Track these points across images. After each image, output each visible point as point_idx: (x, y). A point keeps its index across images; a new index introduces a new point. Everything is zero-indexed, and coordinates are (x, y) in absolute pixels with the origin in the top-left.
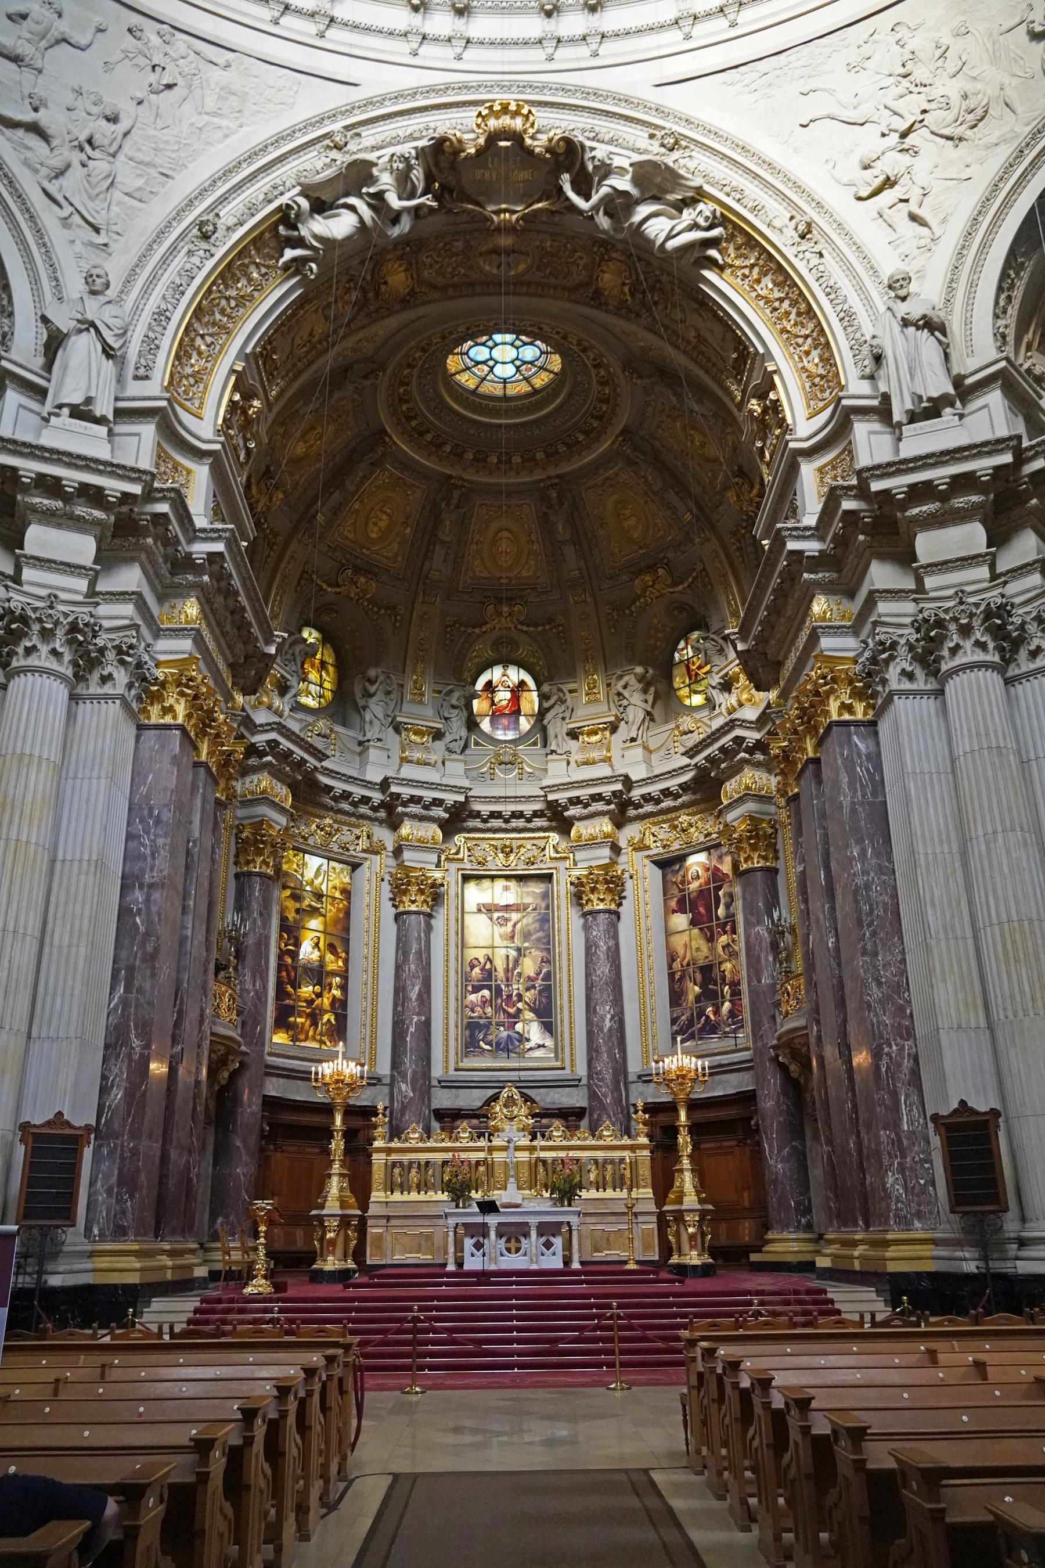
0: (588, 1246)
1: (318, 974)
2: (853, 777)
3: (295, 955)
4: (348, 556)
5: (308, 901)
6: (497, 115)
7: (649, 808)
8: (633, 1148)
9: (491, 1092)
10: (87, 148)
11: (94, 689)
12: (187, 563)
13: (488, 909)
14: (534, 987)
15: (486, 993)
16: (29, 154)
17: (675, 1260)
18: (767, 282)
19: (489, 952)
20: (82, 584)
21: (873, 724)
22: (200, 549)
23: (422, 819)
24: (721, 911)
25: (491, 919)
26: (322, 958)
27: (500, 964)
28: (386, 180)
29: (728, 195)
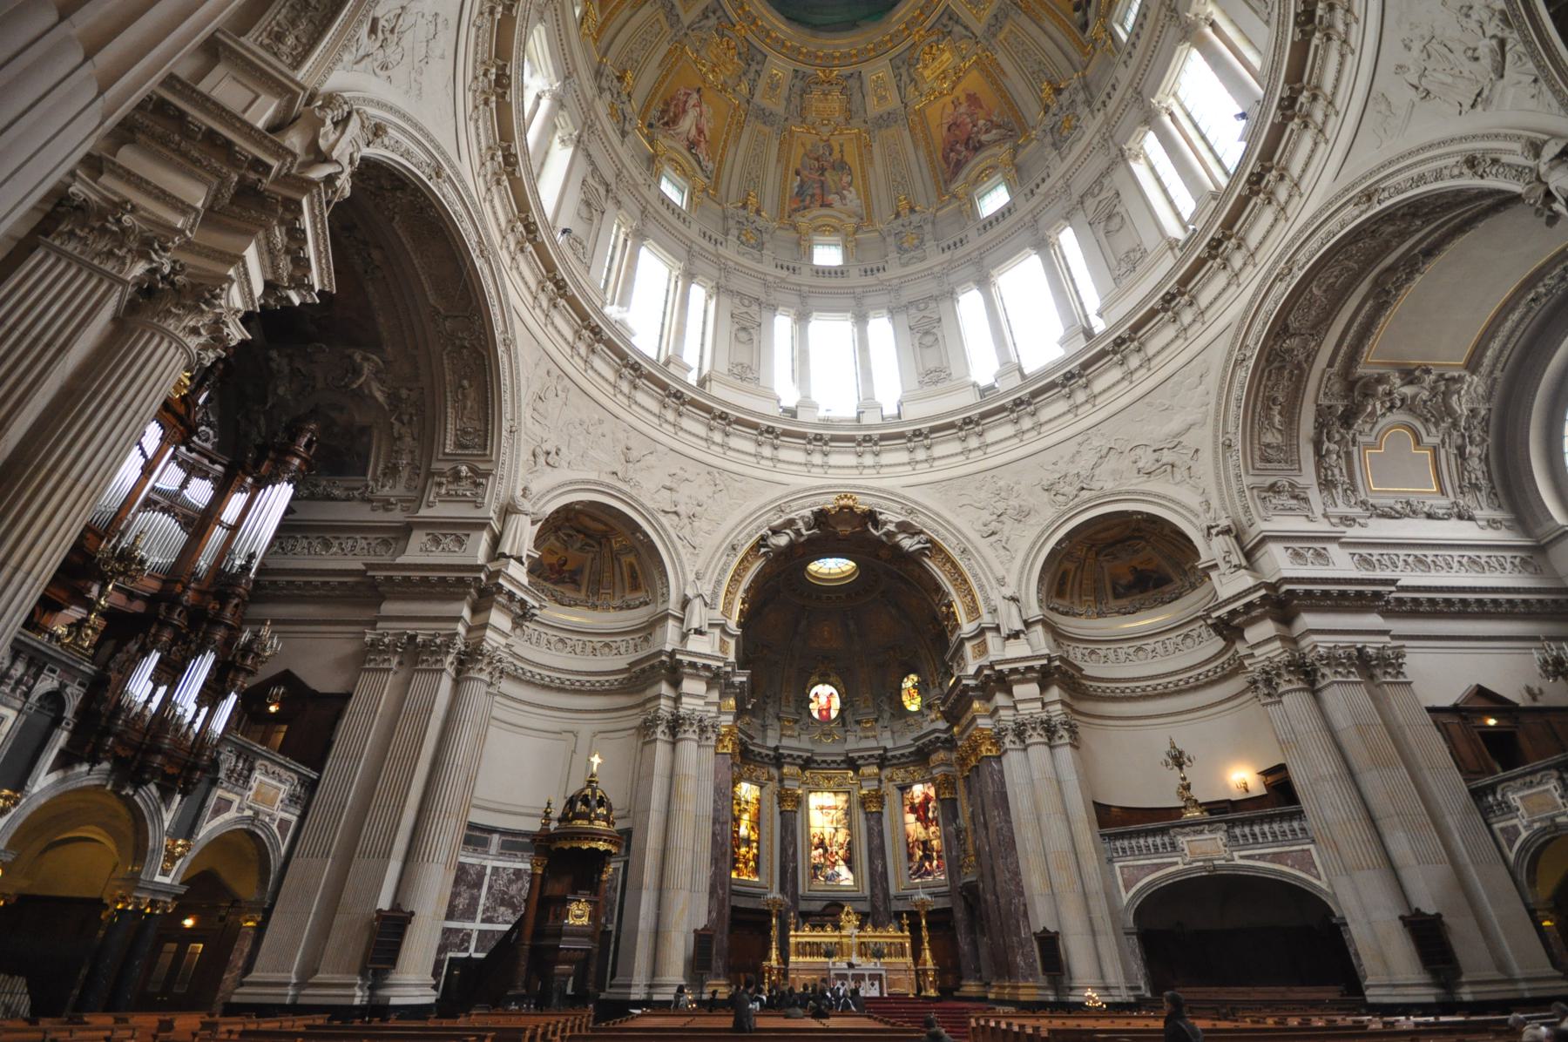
0: (889, 987)
2: (993, 779)
3: (738, 832)
5: (743, 805)
7: (895, 761)
8: (902, 937)
9: (825, 903)
11: (704, 743)
12: (732, 685)
13: (822, 808)
15: (821, 850)
17: (923, 994)
18: (948, 565)
20: (702, 702)
21: (999, 758)
24: (930, 815)
28: (800, 524)
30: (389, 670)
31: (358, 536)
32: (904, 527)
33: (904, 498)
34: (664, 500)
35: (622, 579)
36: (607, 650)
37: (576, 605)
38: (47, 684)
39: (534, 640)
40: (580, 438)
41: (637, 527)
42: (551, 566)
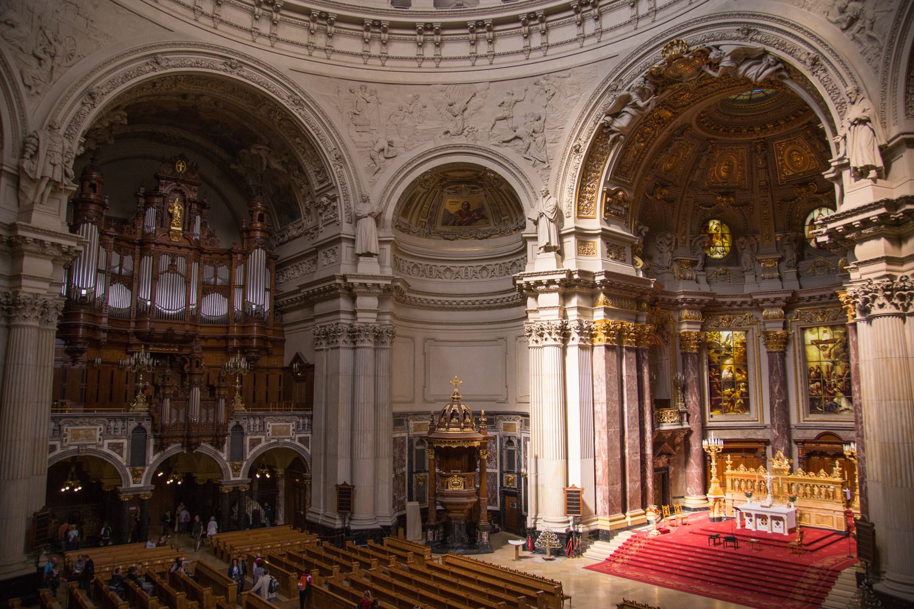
1: (732, 383)
3: (719, 377)
4: (715, 190)
6: (671, 48)
9: (822, 431)
10: (534, 134)
13: (817, 343)
14: (842, 380)
15: (818, 384)
16: (517, 147)
19: (818, 364)
22: (598, 279)
23: (772, 307)
25: (818, 347)
26: (733, 376)
27: (824, 370)
28: (634, 97)
29: (778, 49)
30: (322, 350)
31: (297, 264)
32: (742, 56)
33: (739, 15)
34: (504, 130)
35: (511, 204)
36: (515, 267)
37: (490, 236)
38: (133, 424)
39: (463, 276)
40: (406, 120)
41: (484, 168)
42: (460, 212)
